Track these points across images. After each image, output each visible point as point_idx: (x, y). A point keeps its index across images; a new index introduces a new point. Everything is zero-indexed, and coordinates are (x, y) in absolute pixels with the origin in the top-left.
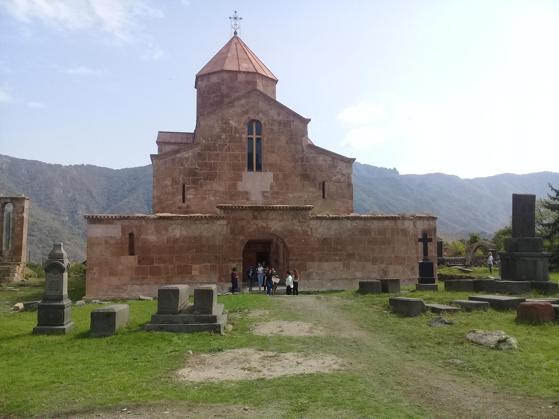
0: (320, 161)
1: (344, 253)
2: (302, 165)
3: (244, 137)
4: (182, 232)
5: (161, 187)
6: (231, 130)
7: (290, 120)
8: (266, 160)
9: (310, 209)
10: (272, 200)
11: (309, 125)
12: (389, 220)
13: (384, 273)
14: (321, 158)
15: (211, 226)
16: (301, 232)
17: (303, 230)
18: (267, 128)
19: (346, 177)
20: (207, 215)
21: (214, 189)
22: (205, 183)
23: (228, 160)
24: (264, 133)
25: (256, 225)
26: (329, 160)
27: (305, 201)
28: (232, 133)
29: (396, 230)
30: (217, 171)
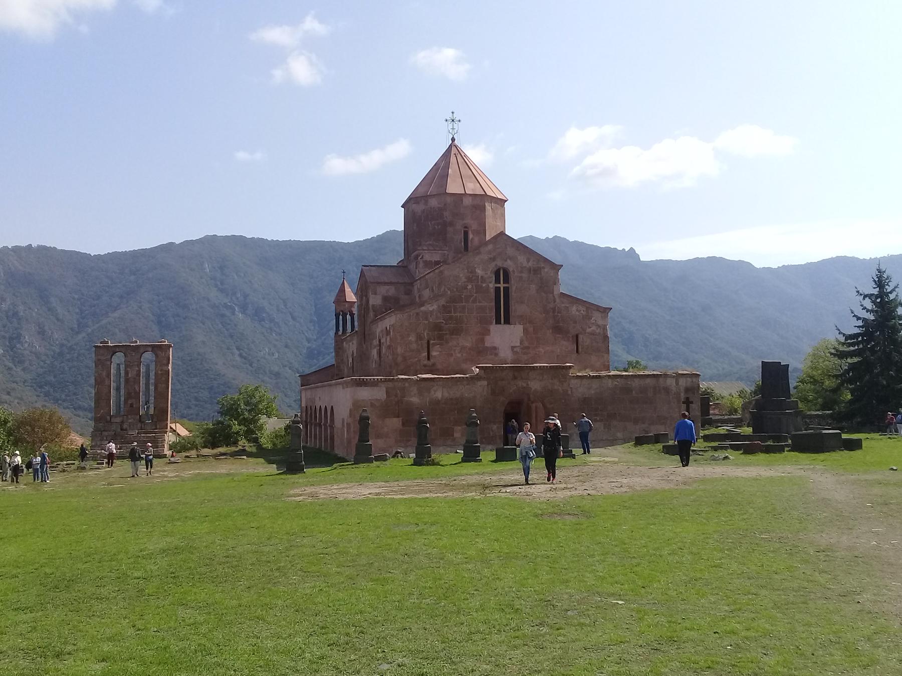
0: (573, 312)
3: (492, 287)
14: (574, 308)
19: (601, 329)
20: (468, 376)
24: (513, 282)
26: (583, 311)
27: (558, 356)
28: (478, 282)
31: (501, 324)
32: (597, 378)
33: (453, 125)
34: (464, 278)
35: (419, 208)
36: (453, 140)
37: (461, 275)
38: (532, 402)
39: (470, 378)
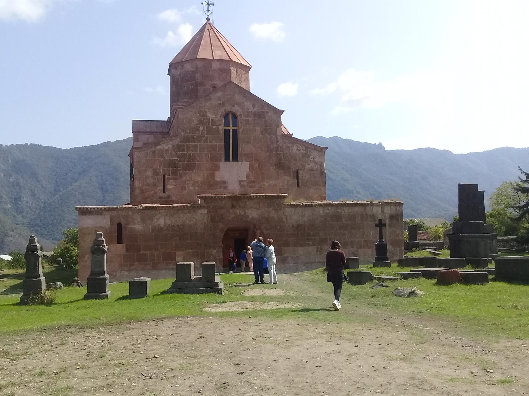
2: (277, 154)
3: (221, 129)
5: (142, 179)
6: (209, 123)
7: (265, 112)
8: (242, 150)
9: (284, 197)
11: (283, 116)
12: (358, 206)
14: (295, 148)
16: (277, 219)
18: (242, 120)
19: (319, 165)
20: (189, 204)
21: (193, 179)
22: (184, 174)
23: (206, 151)
24: (240, 124)
25: (235, 214)
26: (303, 149)
27: (280, 189)
30: (196, 162)
31: (230, 161)
32: (310, 207)
33: (208, 8)
35: (177, 72)
36: (208, 19)
37: (193, 118)
38: (257, 229)
39: (191, 207)
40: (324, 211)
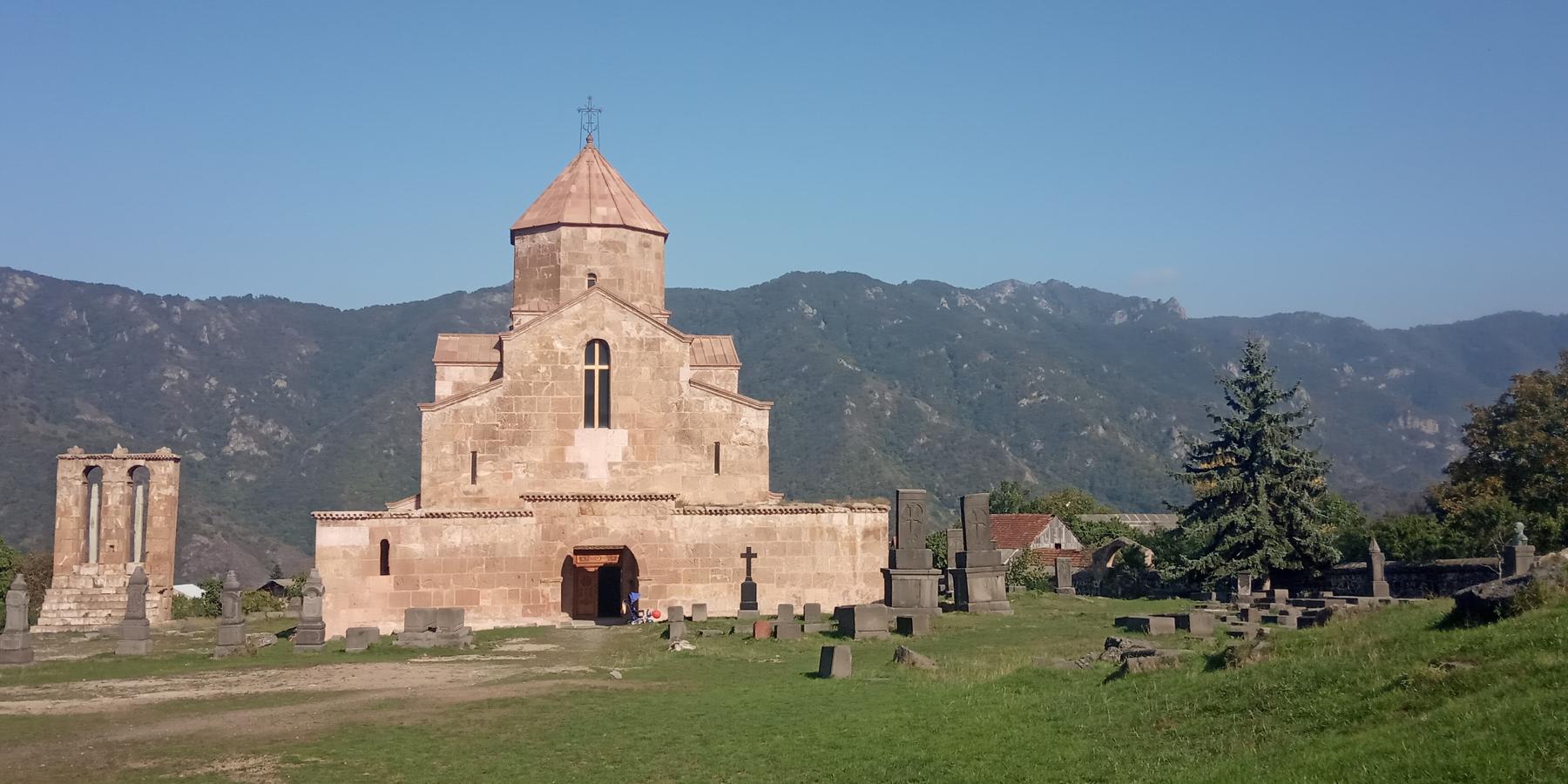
1: (731, 569)
2: (680, 415)
4: (465, 538)
5: (435, 460)
6: (557, 360)
10: (624, 477)
13: (796, 601)
15: (511, 527)
16: (659, 535)
17: (661, 532)
18: (618, 353)
24: (612, 362)
25: (585, 524)
27: (683, 477)
29: (818, 530)
34: (532, 356)
40: (743, 522)
